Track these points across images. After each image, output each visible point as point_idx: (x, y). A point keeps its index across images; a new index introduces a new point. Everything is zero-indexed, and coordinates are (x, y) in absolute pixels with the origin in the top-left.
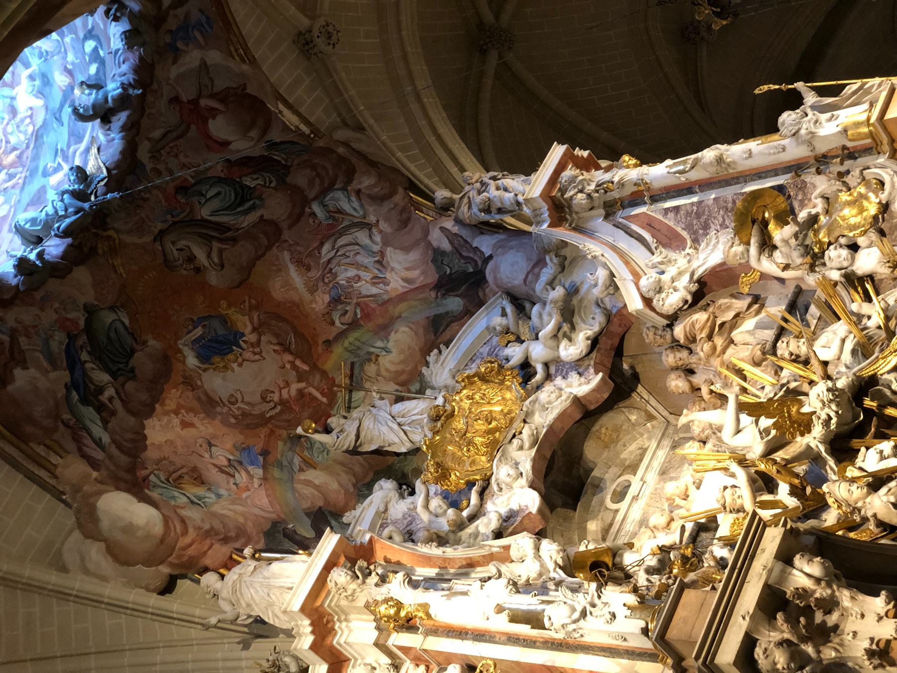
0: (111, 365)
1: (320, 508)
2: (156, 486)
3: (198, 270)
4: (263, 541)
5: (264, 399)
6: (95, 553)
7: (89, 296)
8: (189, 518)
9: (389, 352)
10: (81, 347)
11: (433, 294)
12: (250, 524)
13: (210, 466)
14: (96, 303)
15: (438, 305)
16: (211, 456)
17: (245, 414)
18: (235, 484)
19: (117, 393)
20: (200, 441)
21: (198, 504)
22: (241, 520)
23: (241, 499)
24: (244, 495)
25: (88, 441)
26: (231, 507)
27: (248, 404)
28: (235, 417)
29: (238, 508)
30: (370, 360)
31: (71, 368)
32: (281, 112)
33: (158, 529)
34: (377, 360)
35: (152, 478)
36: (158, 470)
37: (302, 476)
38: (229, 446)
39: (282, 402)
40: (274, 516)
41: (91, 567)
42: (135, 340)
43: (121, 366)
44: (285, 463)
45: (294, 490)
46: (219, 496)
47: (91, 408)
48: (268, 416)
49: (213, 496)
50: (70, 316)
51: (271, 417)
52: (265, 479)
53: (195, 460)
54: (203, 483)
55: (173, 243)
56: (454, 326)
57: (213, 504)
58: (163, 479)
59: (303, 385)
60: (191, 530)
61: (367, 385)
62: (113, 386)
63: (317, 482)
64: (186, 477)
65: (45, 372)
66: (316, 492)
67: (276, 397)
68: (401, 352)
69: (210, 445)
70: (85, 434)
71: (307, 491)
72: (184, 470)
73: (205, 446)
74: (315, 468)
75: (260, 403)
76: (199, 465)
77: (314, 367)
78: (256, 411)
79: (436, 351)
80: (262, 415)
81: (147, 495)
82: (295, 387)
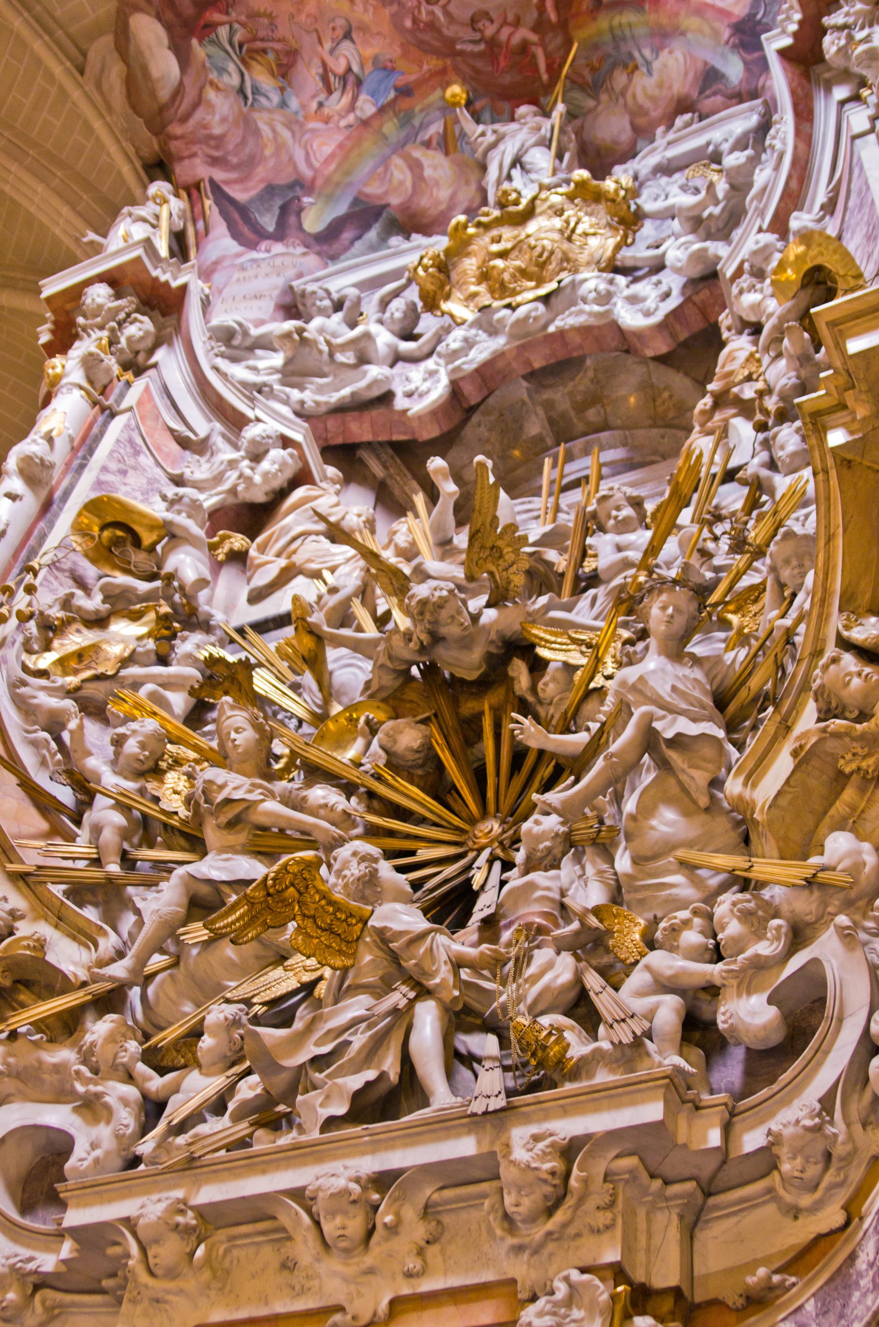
1: (387, 205)
2: (217, 43)
4: (253, 193)
5: (473, 21)
6: (115, 73)
8: (211, 106)
9: (650, 73)
11: (726, 33)
12: (272, 162)
13: (317, 62)
15: (723, 56)
16: (332, 51)
17: (432, 26)
18: (321, 105)
20: (340, 22)
21: (246, 98)
22: (268, 152)
23: (302, 125)
24: (312, 125)
26: (280, 128)
27: (447, 14)
28: (415, 21)
29: (286, 134)
30: (625, 66)
33: (164, 94)
34: (632, 72)
35: (223, 32)
36: (243, 25)
37: (418, 153)
38: (368, 53)
39: (492, 43)
40: (308, 173)
41: (105, 87)
44: (416, 122)
45: (385, 162)
46: (284, 104)
48: (458, 47)
49: (276, 98)
51: (461, 53)
52: (365, 123)
53: (307, 41)
54: (284, 76)
56: (719, 99)
57: (263, 109)
58: (237, 38)
59: (533, 37)
60: (192, 122)
61: (604, 97)
63: (428, 172)
64: (271, 56)
66: (409, 183)
67: (490, 31)
68: (660, 85)
69: (347, 35)
71: (400, 172)
72: (278, 46)
73: (340, 33)
74: (447, 154)
75: (462, 24)
76: (305, 54)
77: (563, 26)
78: (449, 32)
79: (687, 117)
80: (453, 42)
81: (189, 45)
82: (524, 33)
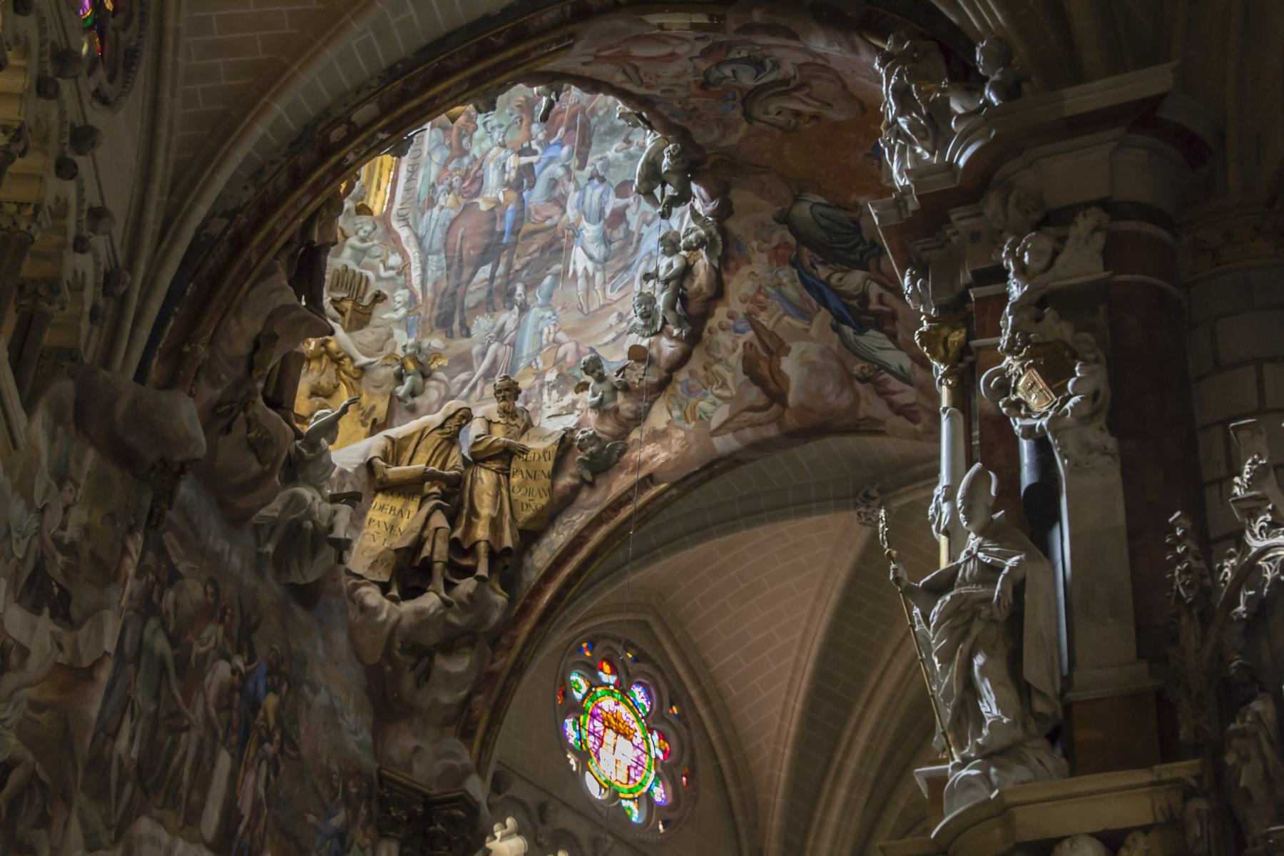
0: (852, 256)
3: (815, 117)
7: (769, 211)
10: (813, 265)
14: (779, 208)
19: (882, 284)
25: (895, 384)
31: (824, 302)
32: (661, 26)
42: (846, 209)
43: (860, 248)
47: (872, 332)
50: (774, 243)
55: (766, 113)
62: (873, 280)
65: (804, 335)
70: (886, 375)
